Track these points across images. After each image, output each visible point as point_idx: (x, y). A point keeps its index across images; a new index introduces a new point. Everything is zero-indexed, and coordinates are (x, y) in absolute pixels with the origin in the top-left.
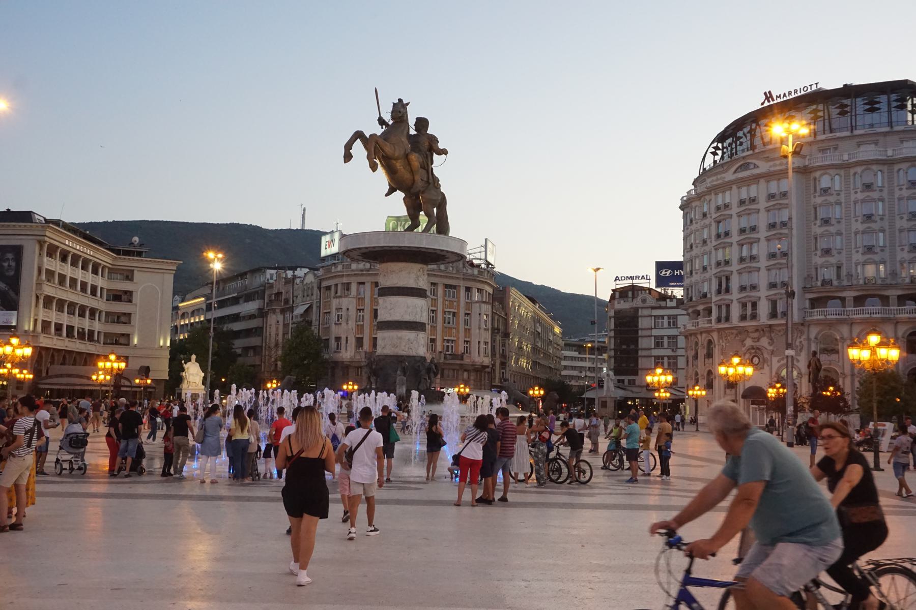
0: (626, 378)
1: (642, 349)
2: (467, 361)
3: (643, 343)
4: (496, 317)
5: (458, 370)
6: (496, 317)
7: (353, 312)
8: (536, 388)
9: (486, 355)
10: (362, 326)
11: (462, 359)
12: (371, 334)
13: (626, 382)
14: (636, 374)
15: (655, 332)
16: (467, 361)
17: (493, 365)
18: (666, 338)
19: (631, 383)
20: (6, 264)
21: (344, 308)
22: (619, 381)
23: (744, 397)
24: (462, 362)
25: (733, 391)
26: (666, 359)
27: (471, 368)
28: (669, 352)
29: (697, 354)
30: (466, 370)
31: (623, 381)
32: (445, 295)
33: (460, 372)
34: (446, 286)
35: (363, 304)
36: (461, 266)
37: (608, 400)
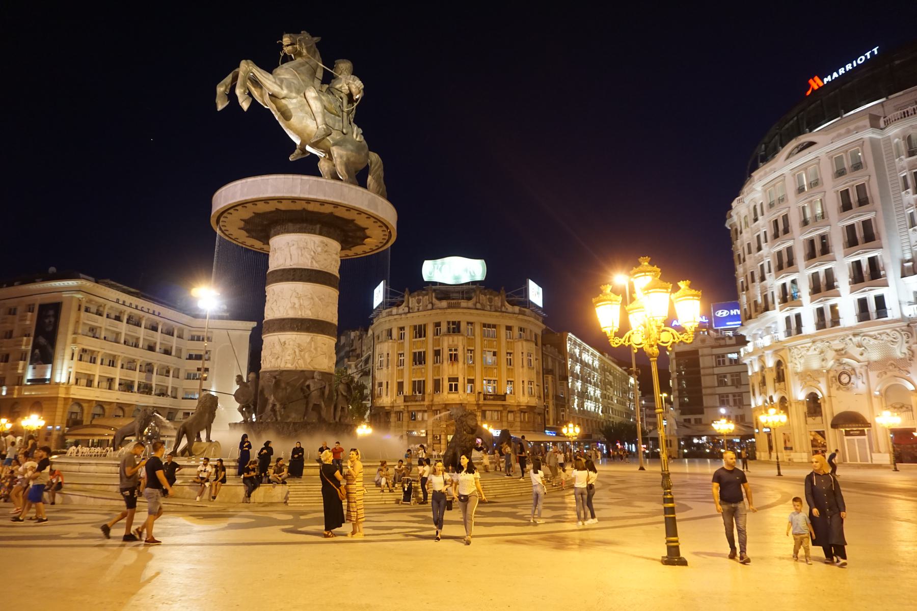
0: (692, 417)
1: (706, 388)
2: (510, 401)
3: (706, 381)
4: (550, 359)
5: (501, 412)
6: (550, 359)
7: (394, 358)
8: (571, 425)
9: (531, 394)
10: (402, 370)
11: (505, 400)
12: (410, 378)
13: (693, 422)
14: (702, 413)
15: (717, 370)
16: (510, 401)
17: (546, 407)
18: (728, 376)
19: (699, 421)
20: (47, 321)
21: (385, 354)
22: (685, 420)
23: (834, 426)
24: (504, 403)
25: (818, 419)
26: (731, 398)
27: (516, 409)
28: (733, 389)
29: (764, 378)
30: (510, 412)
31: (689, 421)
32: (483, 335)
33: (504, 414)
34: (484, 325)
35: (403, 349)
36: (500, 304)
37: (672, 438)
